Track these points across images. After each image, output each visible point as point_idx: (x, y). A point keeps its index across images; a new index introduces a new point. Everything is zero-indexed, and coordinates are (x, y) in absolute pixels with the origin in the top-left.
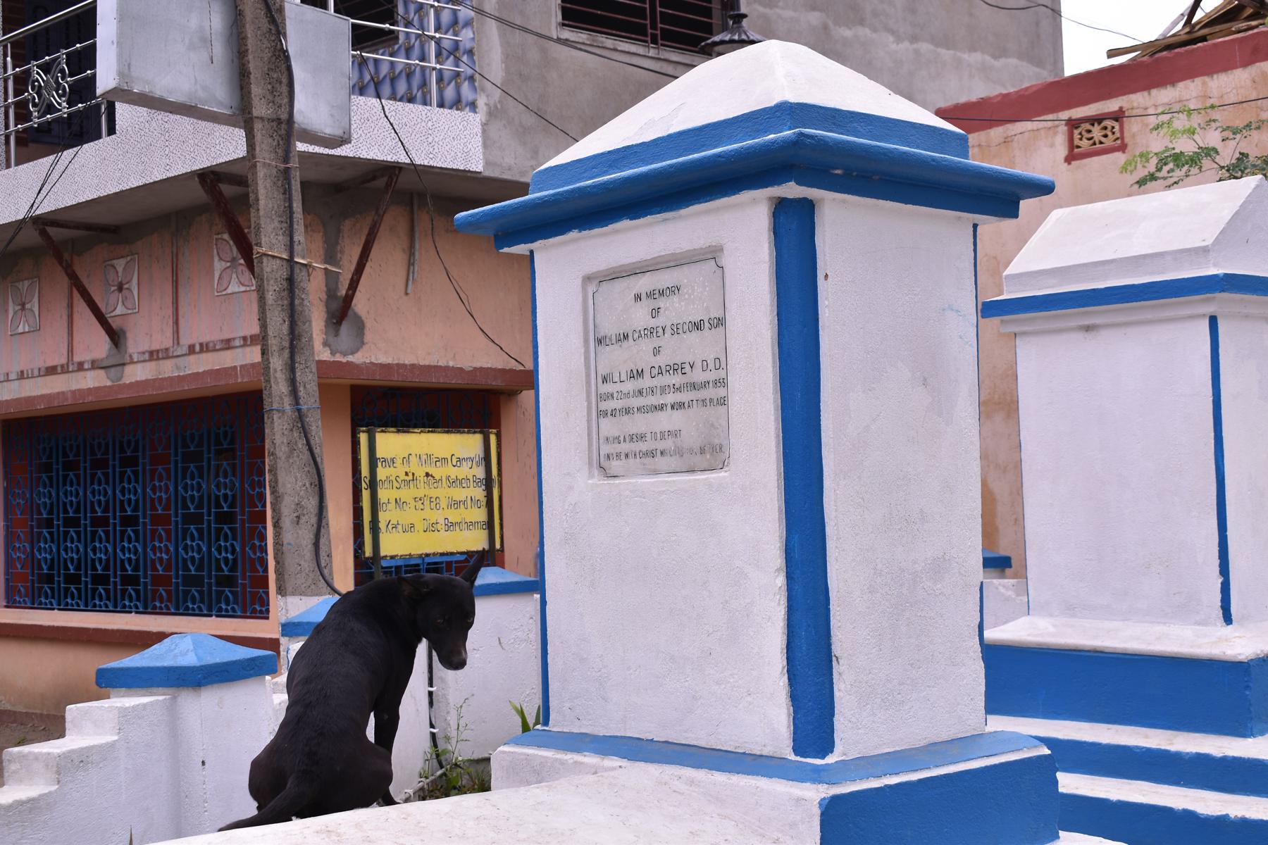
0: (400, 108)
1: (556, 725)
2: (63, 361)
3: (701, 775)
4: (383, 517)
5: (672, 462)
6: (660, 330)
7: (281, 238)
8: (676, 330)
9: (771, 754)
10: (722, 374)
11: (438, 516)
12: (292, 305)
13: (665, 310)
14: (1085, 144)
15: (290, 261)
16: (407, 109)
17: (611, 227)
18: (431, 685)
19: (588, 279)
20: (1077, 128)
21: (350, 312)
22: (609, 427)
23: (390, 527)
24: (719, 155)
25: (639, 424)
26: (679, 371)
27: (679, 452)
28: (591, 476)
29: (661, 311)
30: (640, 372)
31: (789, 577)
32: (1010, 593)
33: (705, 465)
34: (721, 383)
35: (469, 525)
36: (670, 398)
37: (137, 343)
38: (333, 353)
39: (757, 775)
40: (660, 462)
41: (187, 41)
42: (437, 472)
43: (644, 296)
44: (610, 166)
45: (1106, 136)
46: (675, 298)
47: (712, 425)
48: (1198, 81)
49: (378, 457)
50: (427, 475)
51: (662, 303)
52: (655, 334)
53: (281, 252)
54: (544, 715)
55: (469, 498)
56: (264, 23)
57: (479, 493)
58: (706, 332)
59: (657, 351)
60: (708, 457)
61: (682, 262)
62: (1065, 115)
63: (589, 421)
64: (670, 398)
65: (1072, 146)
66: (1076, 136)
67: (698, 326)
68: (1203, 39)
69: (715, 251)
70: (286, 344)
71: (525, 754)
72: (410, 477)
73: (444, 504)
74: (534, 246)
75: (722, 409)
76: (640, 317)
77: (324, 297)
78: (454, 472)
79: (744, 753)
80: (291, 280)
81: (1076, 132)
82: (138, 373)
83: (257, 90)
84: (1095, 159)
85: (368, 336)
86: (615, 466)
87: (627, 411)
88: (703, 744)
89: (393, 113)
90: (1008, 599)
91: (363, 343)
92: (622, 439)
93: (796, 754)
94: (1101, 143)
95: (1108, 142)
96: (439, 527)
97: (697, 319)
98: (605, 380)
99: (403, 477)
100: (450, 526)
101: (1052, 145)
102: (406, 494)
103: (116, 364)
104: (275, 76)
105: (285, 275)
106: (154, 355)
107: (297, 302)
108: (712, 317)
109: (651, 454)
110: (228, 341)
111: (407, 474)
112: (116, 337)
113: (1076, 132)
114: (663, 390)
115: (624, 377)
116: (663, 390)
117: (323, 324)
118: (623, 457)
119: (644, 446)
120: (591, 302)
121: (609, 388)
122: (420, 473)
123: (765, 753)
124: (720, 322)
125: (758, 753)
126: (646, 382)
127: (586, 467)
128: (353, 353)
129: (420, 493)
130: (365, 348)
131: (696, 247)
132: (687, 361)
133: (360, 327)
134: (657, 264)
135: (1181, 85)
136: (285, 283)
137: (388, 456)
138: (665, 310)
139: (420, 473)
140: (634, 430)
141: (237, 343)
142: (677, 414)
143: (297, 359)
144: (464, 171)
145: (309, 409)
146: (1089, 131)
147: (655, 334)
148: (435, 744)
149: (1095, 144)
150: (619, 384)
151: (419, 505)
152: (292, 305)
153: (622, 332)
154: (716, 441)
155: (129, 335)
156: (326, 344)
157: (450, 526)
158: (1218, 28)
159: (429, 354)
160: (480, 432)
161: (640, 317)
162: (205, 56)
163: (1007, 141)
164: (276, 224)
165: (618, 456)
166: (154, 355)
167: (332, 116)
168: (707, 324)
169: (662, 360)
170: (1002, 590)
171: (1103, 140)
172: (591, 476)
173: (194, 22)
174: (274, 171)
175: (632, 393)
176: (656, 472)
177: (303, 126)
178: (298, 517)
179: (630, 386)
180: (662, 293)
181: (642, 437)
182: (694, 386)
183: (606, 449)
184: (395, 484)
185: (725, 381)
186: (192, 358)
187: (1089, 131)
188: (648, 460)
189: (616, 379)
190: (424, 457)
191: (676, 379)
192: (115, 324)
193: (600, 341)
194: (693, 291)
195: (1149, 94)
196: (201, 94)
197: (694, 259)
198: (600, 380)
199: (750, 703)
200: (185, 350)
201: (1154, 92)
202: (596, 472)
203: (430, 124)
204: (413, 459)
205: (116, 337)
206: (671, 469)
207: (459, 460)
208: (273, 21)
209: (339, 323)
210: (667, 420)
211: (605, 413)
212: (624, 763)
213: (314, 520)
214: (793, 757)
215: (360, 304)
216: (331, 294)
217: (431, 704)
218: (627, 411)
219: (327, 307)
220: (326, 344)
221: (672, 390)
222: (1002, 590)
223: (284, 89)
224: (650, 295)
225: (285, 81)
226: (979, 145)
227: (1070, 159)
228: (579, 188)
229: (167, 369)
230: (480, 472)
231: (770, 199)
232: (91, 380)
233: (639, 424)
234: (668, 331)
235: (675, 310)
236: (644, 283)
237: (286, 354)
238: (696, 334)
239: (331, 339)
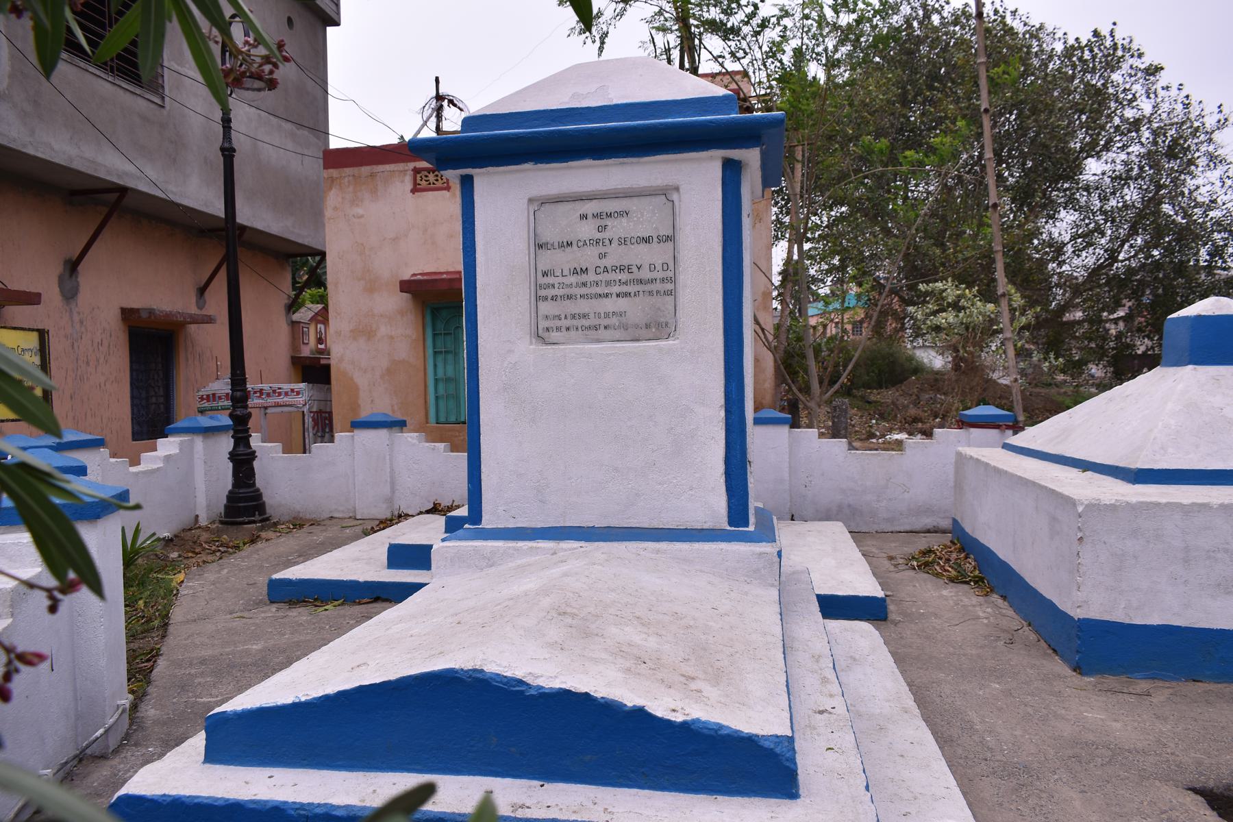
1: (487, 522)
3: (663, 545)
5: (617, 334)
6: (607, 242)
8: (623, 242)
9: (711, 527)
10: (671, 274)
13: (612, 228)
14: (424, 183)
17: (571, 163)
19: (531, 200)
20: (419, 173)
22: (545, 308)
24: (711, 121)
25: (583, 306)
26: (626, 271)
27: (625, 327)
28: (531, 343)
29: (608, 228)
30: (584, 269)
31: (727, 411)
32: (415, 441)
33: (651, 336)
34: (673, 280)
36: (616, 289)
39: (717, 541)
40: (602, 331)
43: (590, 216)
44: (553, 120)
45: (437, 180)
46: (624, 220)
47: (659, 309)
51: (609, 222)
52: (601, 244)
54: (476, 514)
58: (655, 244)
59: (602, 256)
60: (654, 330)
61: (631, 194)
62: (411, 165)
63: (530, 303)
64: (616, 289)
65: (415, 183)
66: (418, 178)
67: (647, 240)
69: (667, 190)
71: (472, 546)
74: (477, 170)
75: (670, 299)
76: (587, 230)
79: (686, 529)
81: (418, 176)
84: (430, 192)
86: (554, 335)
87: (569, 297)
88: (646, 526)
90: (414, 445)
92: (563, 317)
93: (731, 526)
94: (434, 184)
95: (439, 184)
97: (646, 235)
98: (545, 274)
101: (403, 182)
108: (661, 234)
109: (596, 328)
113: (418, 176)
114: (608, 283)
115: (566, 272)
116: (608, 283)
118: (563, 329)
119: (586, 323)
120: (532, 217)
121: (550, 280)
123: (704, 527)
124: (670, 238)
125: (699, 528)
126: (591, 277)
127: (528, 336)
131: (654, 185)
132: (634, 264)
134: (605, 194)
138: (612, 228)
140: (576, 311)
142: (620, 299)
146: (426, 176)
147: (601, 244)
149: (430, 184)
150: (560, 278)
153: (565, 241)
154: (662, 320)
161: (587, 230)
163: (372, 175)
165: (559, 329)
168: (655, 240)
169: (608, 262)
170: (409, 439)
171: (435, 182)
172: (531, 343)
175: (574, 284)
176: (599, 341)
179: (573, 279)
180: (609, 215)
181: (585, 316)
182: (641, 282)
183: (543, 324)
185: (673, 279)
187: (426, 176)
188: (592, 333)
189: (558, 273)
191: (624, 276)
193: (540, 246)
194: (642, 215)
197: (643, 193)
198: (540, 274)
199: (692, 495)
202: (534, 340)
206: (615, 339)
207: (23, 350)
210: (609, 305)
211: (546, 298)
212: (582, 543)
214: (729, 528)
218: (569, 297)
221: (618, 283)
222: (409, 439)
224: (597, 216)
226: (354, 175)
227: (414, 191)
228: (560, 131)
231: (723, 158)
233: (583, 306)
234: (615, 243)
235: (618, 228)
236: (591, 207)
238: (643, 247)
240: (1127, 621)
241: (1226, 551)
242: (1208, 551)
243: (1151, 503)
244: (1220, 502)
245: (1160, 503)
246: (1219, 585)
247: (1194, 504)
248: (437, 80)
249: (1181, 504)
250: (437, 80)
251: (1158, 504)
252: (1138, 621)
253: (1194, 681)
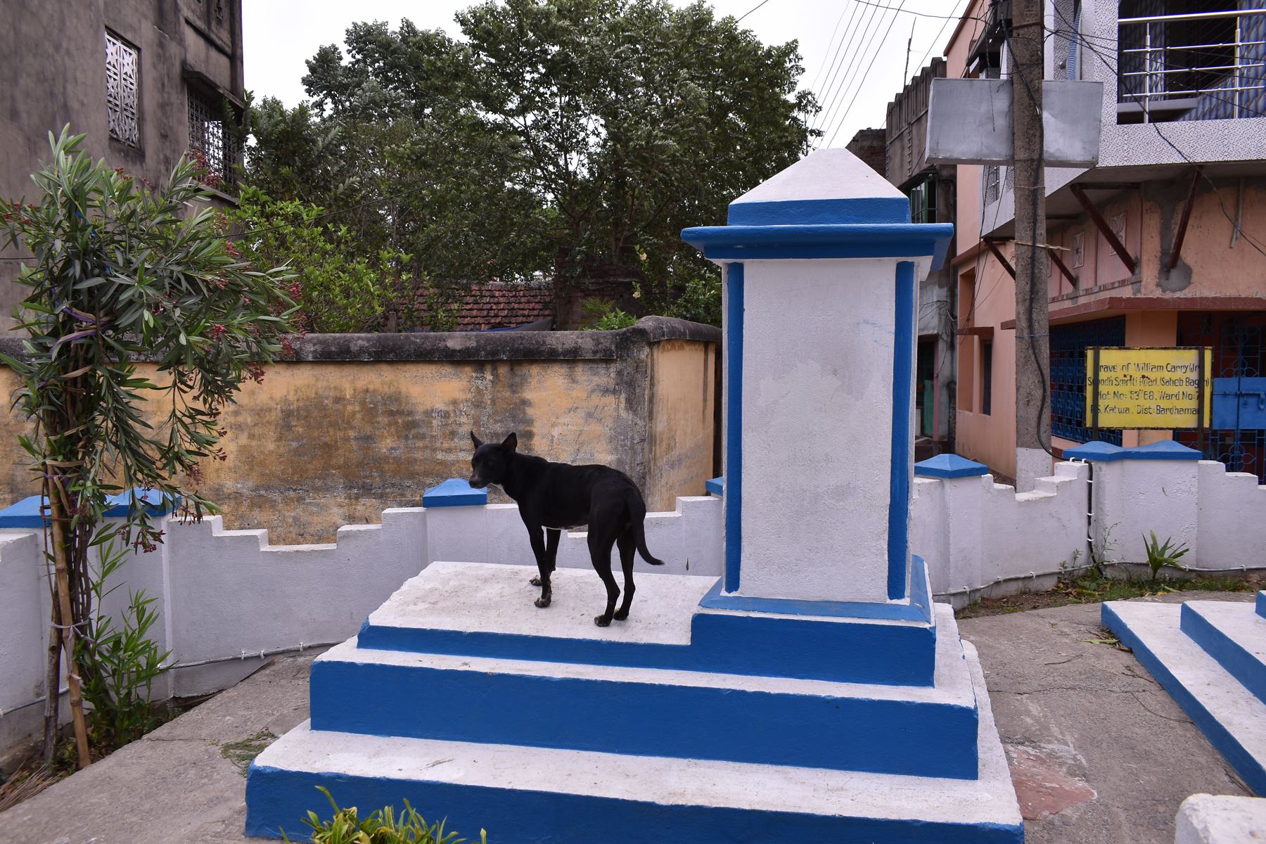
0: (1199, 125)
2: (1057, 294)
4: (1102, 403)
7: (1028, 233)
11: (1152, 404)
12: (1033, 273)
15: (1034, 247)
16: (1205, 125)
18: (1090, 512)
21: (1179, 263)
23: (1108, 409)
35: (1180, 411)
37: (1086, 282)
38: (1164, 291)
41: (978, 121)
42: (1152, 375)
49: (1101, 364)
50: (1143, 377)
53: (1027, 241)
55: (1181, 393)
56: (1026, 101)
57: (1193, 390)
70: (1028, 297)
72: (1128, 378)
73: (1157, 395)
77: (1159, 254)
78: (1167, 376)
80: (1033, 258)
82: (1082, 301)
83: (1018, 143)
85: (1195, 278)
89: (1193, 129)
91: (1190, 283)
96: (1151, 411)
99: (1122, 377)
100: (1160, 410)
102: (1122, 389)
103: (1074, 298)
104: (1032, 132)
105: (1030, 255)
106: (1088, 292)
107: (1036, 271)
110: (1113, 283)
111: (1125, 376)
112: (1074, 281)
117: (1156, 272)
122: (1137, 375)
128: (1180, 290)
129: (1136, 388)
130: (1191, 286)
133: (1188, 272)
136: (1029, 260)
137: (1110, 364)
139: (1137, 375)
141: (1116, 285)
143: (1034, 305)
144: (1257, 160)
145: (1040, 337)
148: (1091, 550)
151: (1135, 396)
152: (1033, 273)
155: (1080, 279)
156: (1158, 285)
157: (1160, 410)
159: (1249, 287)
160: (1196, 349)
162: (990, 127)
164: (1026, 224)
166: (1088, 292)
167: (1084, 148)
173: (984, 108)
174: (1027, 192)
177: (1060, 159)
178: (1029, 401)
184: (1115, 382)
186: (1101, 293)
190: (1141, 366)
192: (1073, 274)
196: (985, 151)
200: (1097, 289)
203: (1126, 147)
204: (1132, 367)
205: (1074, 281)
208: (1032, 98)
209: (1168, 271)
213: (1039, 403)
215: (1188, 255)
216: (1164, 253)
217: (1089, 523)
219: (1161, 261)
220: (1158, 285)
223: (1037, 140)
225: (1038, 134)
229: (1092, 298)
230: (1194, 376)
232: (1067, 304)
237: (1027, 303)
239: (1163, 282)
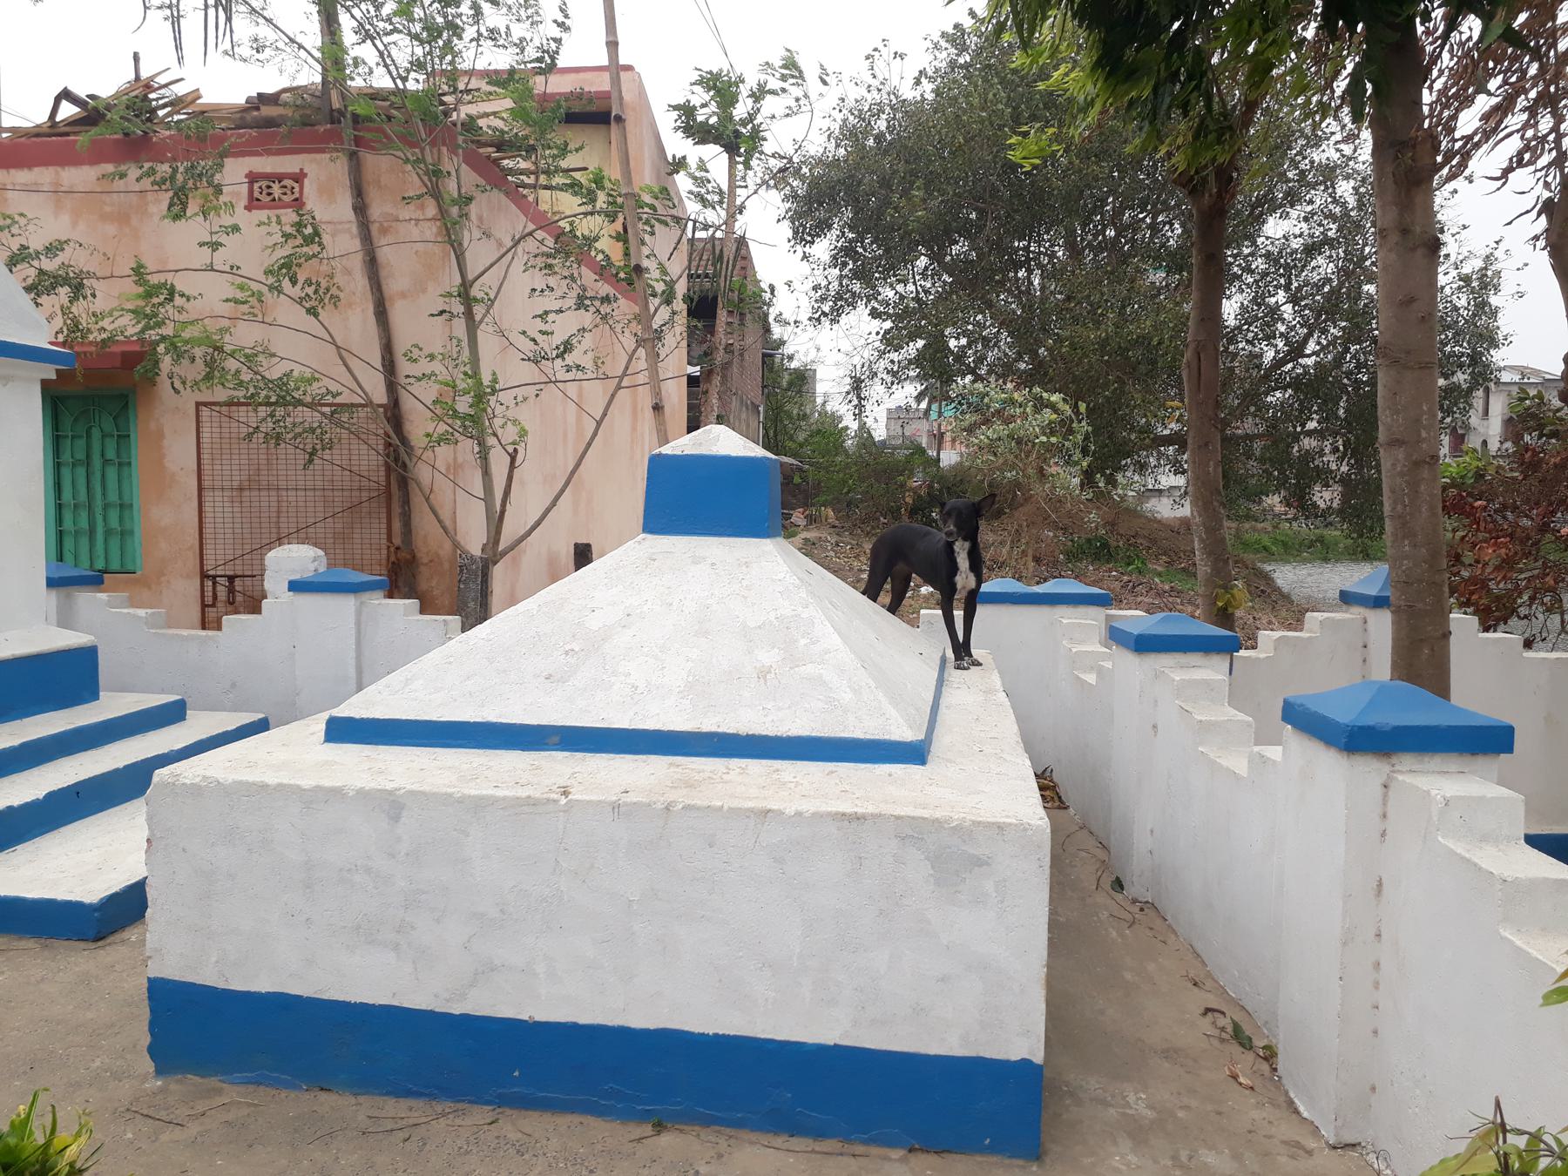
48: (51, 169)
68: (67, 134)
135: (36, 170)
158: (77, 129)
195: (8, 173)
201: (13, 171)
240: (221, 985)
241: (368, 870)
242: (341, 870)
243: (254, 784)
244: (359, 785)
245: (267, 786)
246: (359, 927)
247: (318, 788)
248: (136, 57)
249: (298, 787)
250: (136, 57)
251: (264, 787)
252: (238, 985)
253: (322, 1089)
